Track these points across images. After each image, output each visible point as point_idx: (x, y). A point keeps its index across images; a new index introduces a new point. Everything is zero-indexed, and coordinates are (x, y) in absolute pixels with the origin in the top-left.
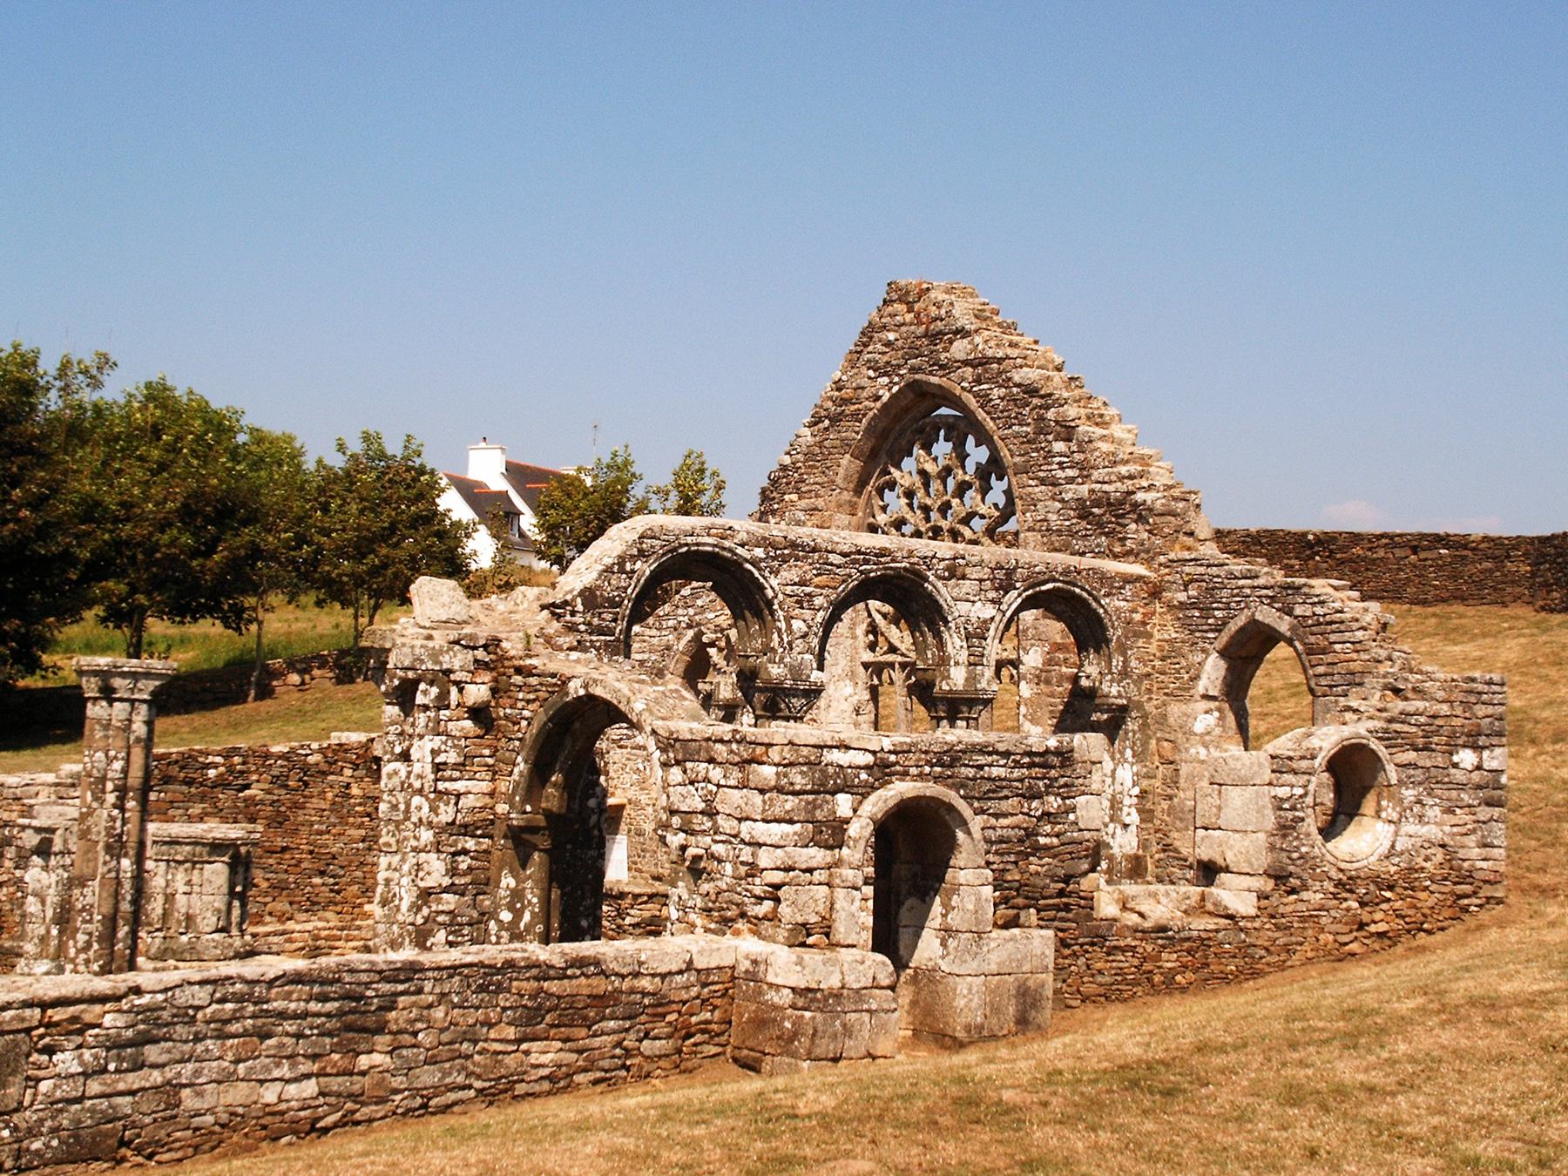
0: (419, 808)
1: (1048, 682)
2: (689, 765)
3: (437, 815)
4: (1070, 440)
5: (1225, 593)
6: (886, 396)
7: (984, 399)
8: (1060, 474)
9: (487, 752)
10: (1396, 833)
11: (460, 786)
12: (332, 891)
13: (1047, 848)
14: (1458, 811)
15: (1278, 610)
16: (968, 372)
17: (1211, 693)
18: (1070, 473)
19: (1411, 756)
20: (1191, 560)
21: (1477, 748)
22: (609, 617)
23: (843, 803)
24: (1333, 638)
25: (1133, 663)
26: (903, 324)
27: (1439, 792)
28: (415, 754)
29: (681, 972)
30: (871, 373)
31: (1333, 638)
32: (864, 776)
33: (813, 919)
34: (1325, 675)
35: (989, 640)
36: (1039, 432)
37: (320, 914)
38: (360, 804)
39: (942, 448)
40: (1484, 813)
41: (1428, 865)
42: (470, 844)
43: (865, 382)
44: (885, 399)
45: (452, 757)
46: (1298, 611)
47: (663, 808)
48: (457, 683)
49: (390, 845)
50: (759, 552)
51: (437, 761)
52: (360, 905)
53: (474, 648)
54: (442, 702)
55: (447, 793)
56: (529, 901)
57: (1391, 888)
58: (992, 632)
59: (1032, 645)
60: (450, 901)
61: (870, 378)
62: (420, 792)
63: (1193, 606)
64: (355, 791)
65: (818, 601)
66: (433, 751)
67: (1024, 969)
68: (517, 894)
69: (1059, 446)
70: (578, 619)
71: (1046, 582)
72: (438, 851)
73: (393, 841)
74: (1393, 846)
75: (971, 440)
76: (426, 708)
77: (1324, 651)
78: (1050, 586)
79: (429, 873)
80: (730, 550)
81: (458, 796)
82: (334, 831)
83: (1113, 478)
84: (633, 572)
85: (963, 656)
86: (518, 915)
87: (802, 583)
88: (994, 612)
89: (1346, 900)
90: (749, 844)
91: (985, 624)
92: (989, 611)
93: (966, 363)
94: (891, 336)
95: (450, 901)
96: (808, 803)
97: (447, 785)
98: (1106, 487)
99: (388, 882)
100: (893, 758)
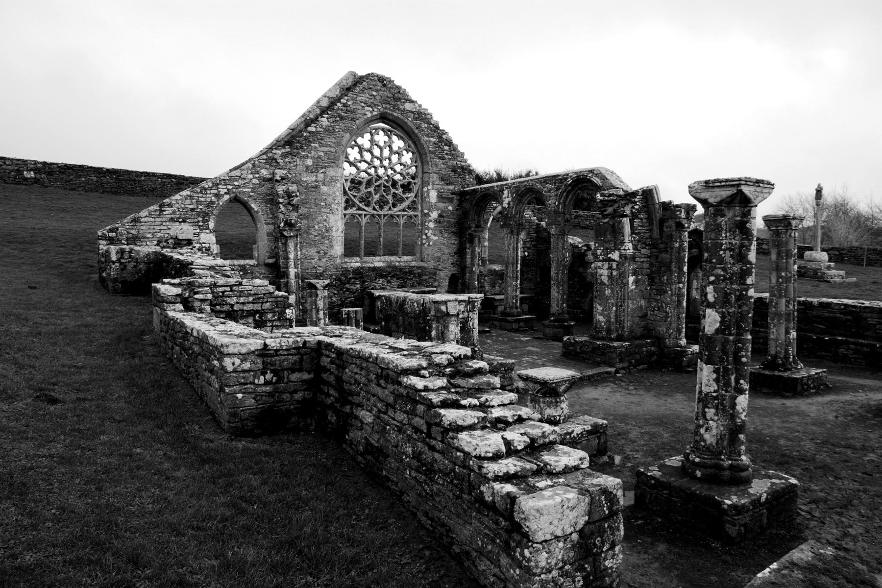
6: (369, 115)
8: (446, 156)
26: (381, 90)
30: (363, 104)
36: (439, 142)
43: (359, 107)
69: (446, 148)
94: (374, 93)
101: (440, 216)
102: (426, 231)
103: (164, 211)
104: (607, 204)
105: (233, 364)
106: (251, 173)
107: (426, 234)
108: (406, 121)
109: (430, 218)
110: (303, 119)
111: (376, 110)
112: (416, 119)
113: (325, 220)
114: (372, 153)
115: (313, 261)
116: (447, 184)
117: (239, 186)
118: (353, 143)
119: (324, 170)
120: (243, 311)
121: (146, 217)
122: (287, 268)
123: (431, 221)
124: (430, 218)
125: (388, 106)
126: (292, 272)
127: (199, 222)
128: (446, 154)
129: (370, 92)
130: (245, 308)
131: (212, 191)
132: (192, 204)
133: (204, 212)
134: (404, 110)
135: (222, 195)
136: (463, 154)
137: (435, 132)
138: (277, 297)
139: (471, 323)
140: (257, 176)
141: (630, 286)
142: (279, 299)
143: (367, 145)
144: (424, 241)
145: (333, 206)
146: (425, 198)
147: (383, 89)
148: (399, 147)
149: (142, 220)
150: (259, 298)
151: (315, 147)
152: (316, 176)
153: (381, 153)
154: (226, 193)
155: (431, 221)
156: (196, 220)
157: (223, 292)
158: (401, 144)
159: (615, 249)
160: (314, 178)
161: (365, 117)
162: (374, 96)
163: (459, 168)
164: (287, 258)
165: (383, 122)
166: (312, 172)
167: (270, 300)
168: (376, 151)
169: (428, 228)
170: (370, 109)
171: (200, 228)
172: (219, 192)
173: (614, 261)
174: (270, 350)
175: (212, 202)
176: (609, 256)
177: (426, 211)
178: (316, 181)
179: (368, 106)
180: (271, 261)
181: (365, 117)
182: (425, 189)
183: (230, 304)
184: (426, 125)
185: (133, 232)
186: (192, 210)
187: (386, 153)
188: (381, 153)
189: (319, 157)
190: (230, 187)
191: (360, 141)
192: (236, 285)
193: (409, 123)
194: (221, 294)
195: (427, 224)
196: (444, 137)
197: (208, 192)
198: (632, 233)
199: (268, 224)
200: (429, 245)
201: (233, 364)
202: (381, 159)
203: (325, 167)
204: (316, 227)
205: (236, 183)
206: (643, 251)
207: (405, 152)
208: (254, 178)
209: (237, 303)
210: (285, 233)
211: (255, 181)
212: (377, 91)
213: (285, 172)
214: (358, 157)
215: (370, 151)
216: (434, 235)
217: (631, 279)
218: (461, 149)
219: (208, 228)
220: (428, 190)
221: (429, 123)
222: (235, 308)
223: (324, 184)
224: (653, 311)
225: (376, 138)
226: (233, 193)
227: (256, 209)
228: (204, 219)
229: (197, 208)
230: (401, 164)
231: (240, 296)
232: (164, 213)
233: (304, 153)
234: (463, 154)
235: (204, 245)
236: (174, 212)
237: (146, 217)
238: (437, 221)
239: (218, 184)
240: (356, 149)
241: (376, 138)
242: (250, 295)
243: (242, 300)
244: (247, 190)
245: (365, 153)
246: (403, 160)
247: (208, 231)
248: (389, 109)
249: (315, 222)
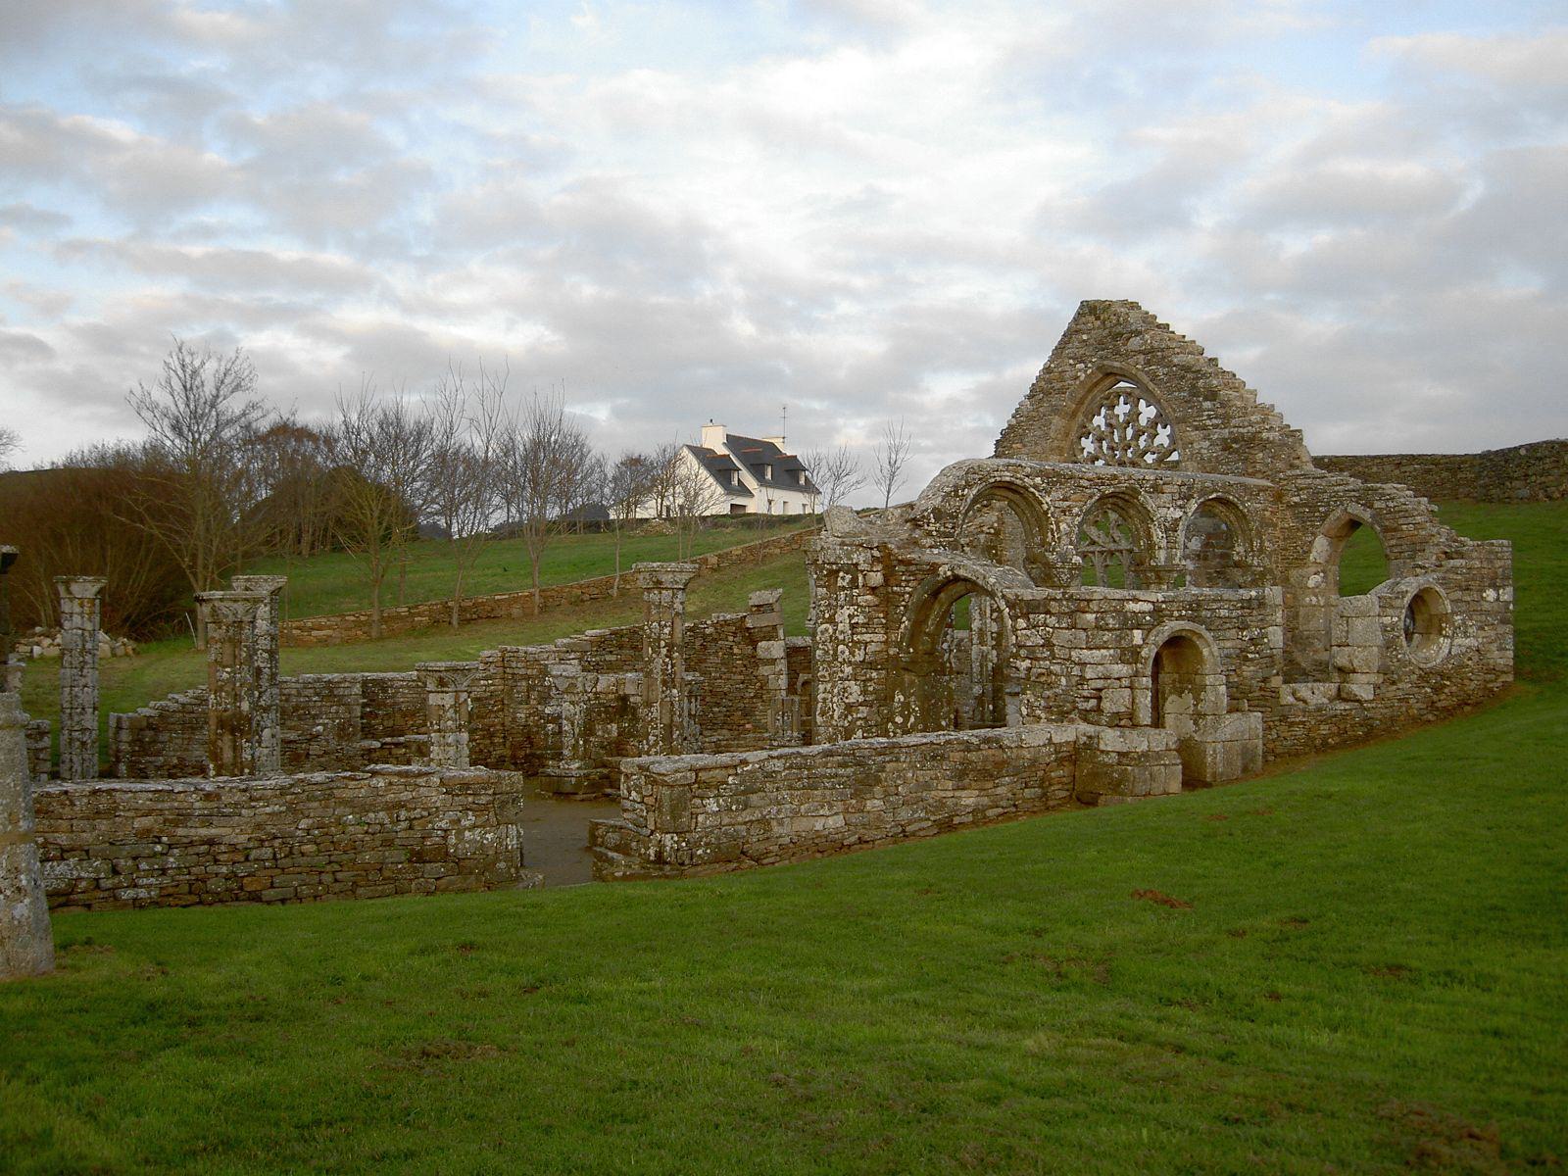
0: (843, 652)
1: (1206, 559)
2: (1031, 616)
3: (854, 656)
4: (1215, 400)
5: (1326, 496)
7: (1154, 378)
8: (1208, 422)
9: (881, 615)
10: (1451, 645)
11: (867, 637)
12: (725, 715)
13: (1252, 660)
14: (1486, 628)
15: (1362, 505)
16: (1141, 357)
17: (1318, 561)
18: (1215, 421)
19: (1458, 594)
20: (1302, 475)
21: (1496, 588)
22: (950, 526)
23: (1137, 636)
24: (1401, 521)
25: (1267, 544)
26: (1094, 329)
27: (1474, 617)
28: (838, 618)
29: (1044, 745)
30: (1071, 361)
31: (1401, 521)
32: (1148, 618)
33: (1123, 709)
34: (1396, 545)
35: (1179, 532)
37: (719, 731)
38: (740, 659)
39: (1122, 409)
40: (1502, 629)
41: (1470, 662)
42: (874, 674)
43: (1067, 368)
44: (1082, 379)
45: (861, 619)
46: (1377, 505)
47: (1013, 644)
48: (862, 571)
49: (825, 677)
50: (1038, 480)
51: (853, 622)
52: (744, 725)
53: (872, 549)
54: (854, 583)
55: (859, 642)
56: (913, 709)
57: (1449, 679)
58: (1180, 527)
59: (1194, 535)
60: (864, 711)
62: (843, 642)
63: (1305, 505)
64: (736, 651)
65: (1076, 510)
66: (849, 616)
67: (1245, 737)
68: (906, 705)
69: (1207, 404)
70: (931, 528)
71: (1212, 493)
72: (856, 680)
73: (826, 674)
74: (1450, 652)
75: (1142, 403)
76: (843, 588)
77: (1395, 530)
78: (1214, 496)
79: (851, 694)
80: (1021, 479)
81: (866, 644)
82: (724, 677)
83: (1246, 424)
84: (963, 495)
85: (1164, 543)
86: (906, 719)
87: (1065, 499)
88: (1181, 514)
89: (1423, 687)
90: (1079, 664)
91: (1177, 521)
92: (1178, 514)
93: (1140, 352)
94: (1085, 337)
95: (864, 711)
96: (1117, 636)
97: (859, 637)
98: (1241, 430)
99: (825, 699)
100: (1164, 606)
101: (1206, 545)
112: (1148, 363)
128: (1209, 418)
134: (1127, 355)
137: (1183, 377)
163: (1235, 441)
170: (1083, 365)
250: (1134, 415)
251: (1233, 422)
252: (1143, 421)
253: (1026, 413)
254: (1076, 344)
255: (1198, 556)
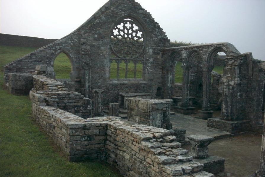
1: (153, 64)
6: (123, 15)
7: (145, 21)
8: (157, 34)
18: (159, 34)
26: (128, 4)
30: (120, 10)
61: (120, 11)
69: (157, 30)
93: (142, 14)
94: (126, 6)
101: (154, 61)
102: (147, 67)
103: (32, 57)
104: (229, 60)
105: (72, 132)
106: (70, 40)
107: (147, 69)
108: (140, 18)
109: (149, 62)
110: (94, 17)
111: (126, 13)
112: (144, 17)
113: (102, 62)
114: (124, 32)
115: (96, 80)
116: (157, 46)
117: (64, 47)
118: (116, 27)
119: (102, 39)
120: (70, 106)
121: (25, 59)
122: (85, 83)
123: (149, 63)
124: (149, 62)
125: (132, 11)
126: (87, 85)
127: (47, 62)
128: (157, 33)
129: (124, 5)
130: (71, 105)
131: (53, 48)
132: (44, 54)
133: (49, 58)
134: (139, 13)
135: (57, 51)
136: (165, 33)
137: (152, 23)
138: (85, 100)
139: (168, 113)
140: (73, 42)
141: (238, 97)
142: (85, 101)
143: (122, 28)
144: (146, 72)
145: (106, 55)
146: (147, 52)
147: (130, 3)
148: (136, 29)
149: (23, 61)
150: (77, 100)
151: (99, 29)
152: (99, 42)
153: (128, 32)
154: (59, 49)
155: (149, 63)
156: (45, 61)
157: (62, 98)
158: (137, 28)
159: (232, 80)
160: (98, 43)
161: (121, 16)
162: (125, 6)
163: (163, 39)
164: (84, 79)
165: (129, 18)
166: (97, 40)
167: (81, 101)
168: (126, 31)
169: (148, 66)
170: (124, 12)
171: (47, 65)
172: (56, 48)
173: (231, 85)
174: (87, 127)
175: (53, 53)
176: (229, 83)
177: (147, 58)
178: (98, 44)
179: (123, 11)
180: (78, 80)
181: (121, 16)
182: (147, 48)
183: (65, 103)
184: (149, 20)
185: (19, 66)
186: (44, 56)
187: (130, 32)
188: (128, 32)
189: (101, 34)
190: (61, 47)
191: (119, 26)
192: (68, 95)
193: (141, 19)
194: (61, 99)
195: (148, 64)
196: (156, 25)
197: (51, 49)
198: (240, 73)
199: (77, 63)
200: (148, 74)
201: (72, 132)
202: (128, 34)
203: (103, 38)
204: (98, 65)
205: (64, 45)
206: (244, 81)
207: (138, 32)
208: (72, 43)
209: (68, 102)
210: (84, 68)
211: (72, 44)
212: (127, 4)
213: (85, 40)
214: (118, 34)
215: (123, 31)
216: (151, 69)
217: (239, 94)
218: (164, 30)
219: (51, 65)
220: (149, 49)
221: (150, 19)
222: (67, 104)
223: (102, 46)
224: (248, 108)
225: (126, 25)
226: (62, 49)
227: (72, 57)
228: (49, 60)
229: (46, 56)
230: (137, 37)
231: (69, 100)
232: (32, 58)
233: (94, 32)
234: (165, 33)
235: (49, 72)
236: (36, 57)
237: (25, 59)
238: (152, 63)
239: (56, 45)
240: (117, 30)
241: (126, 25)
242: (74, 99)
243: (70, 101)
244: (68, 48)
245: (121, 32)
246: (138, 35)
247: (50, 66)
248: (132, 13)
249: (98, 63)
250: (132, 28)
251: (163, 35)
252: (134, 29)
253: (103, 20)
254: (122, 6)
255: (152, 63)
